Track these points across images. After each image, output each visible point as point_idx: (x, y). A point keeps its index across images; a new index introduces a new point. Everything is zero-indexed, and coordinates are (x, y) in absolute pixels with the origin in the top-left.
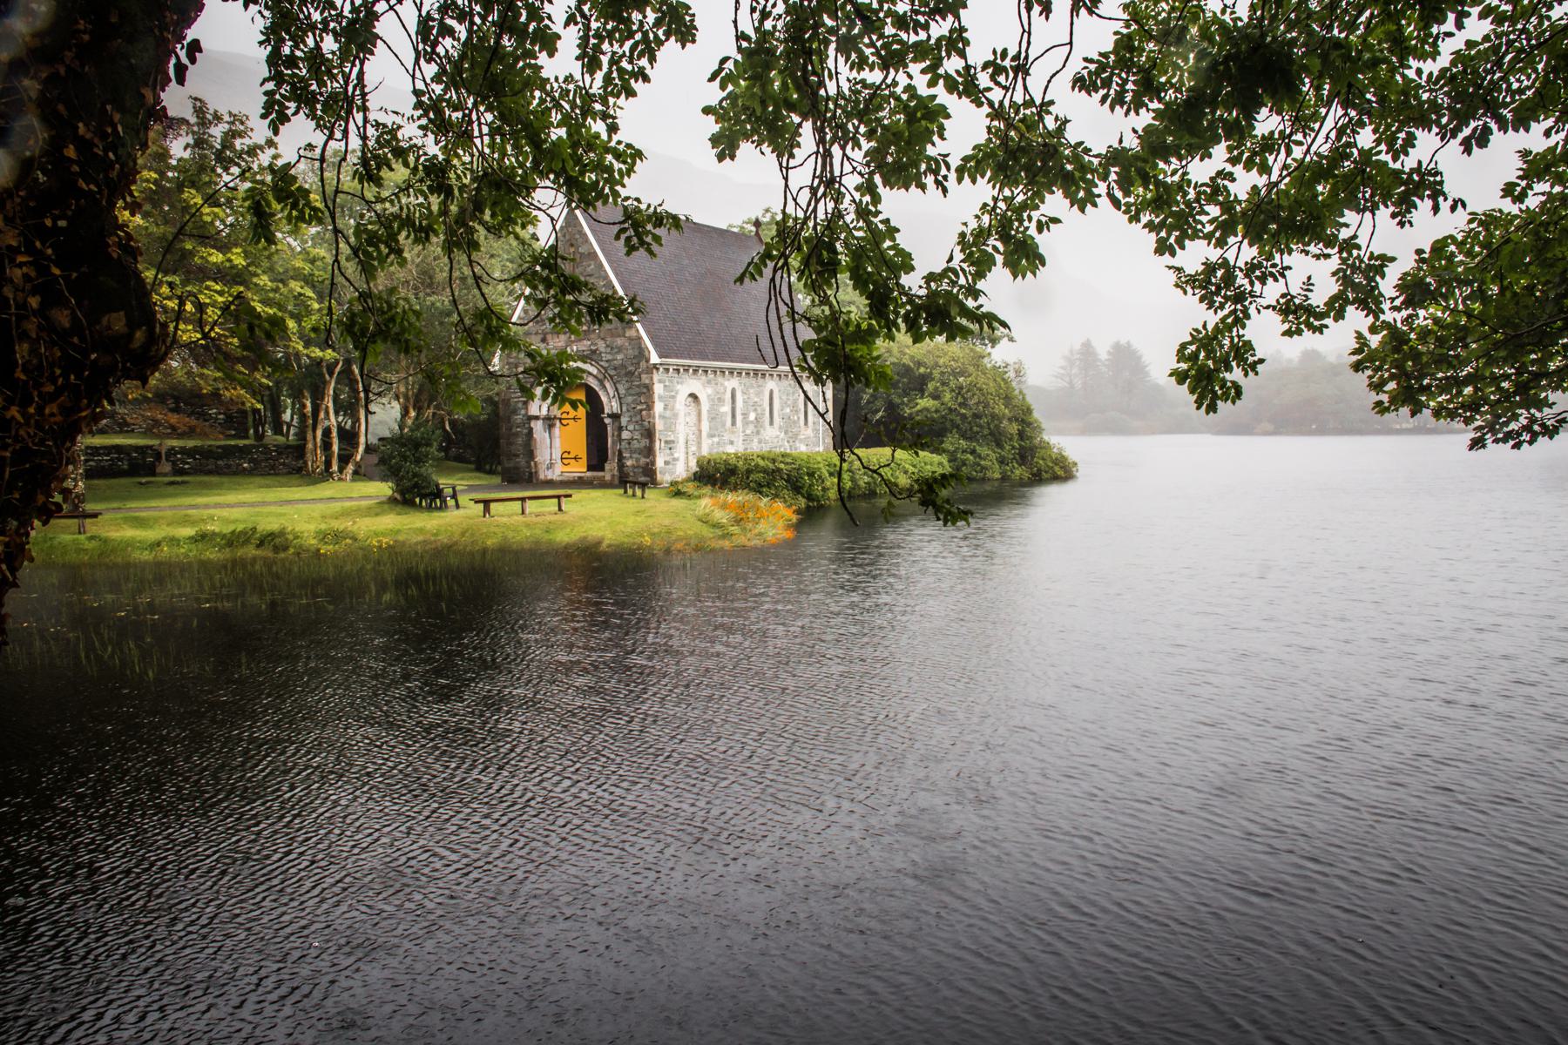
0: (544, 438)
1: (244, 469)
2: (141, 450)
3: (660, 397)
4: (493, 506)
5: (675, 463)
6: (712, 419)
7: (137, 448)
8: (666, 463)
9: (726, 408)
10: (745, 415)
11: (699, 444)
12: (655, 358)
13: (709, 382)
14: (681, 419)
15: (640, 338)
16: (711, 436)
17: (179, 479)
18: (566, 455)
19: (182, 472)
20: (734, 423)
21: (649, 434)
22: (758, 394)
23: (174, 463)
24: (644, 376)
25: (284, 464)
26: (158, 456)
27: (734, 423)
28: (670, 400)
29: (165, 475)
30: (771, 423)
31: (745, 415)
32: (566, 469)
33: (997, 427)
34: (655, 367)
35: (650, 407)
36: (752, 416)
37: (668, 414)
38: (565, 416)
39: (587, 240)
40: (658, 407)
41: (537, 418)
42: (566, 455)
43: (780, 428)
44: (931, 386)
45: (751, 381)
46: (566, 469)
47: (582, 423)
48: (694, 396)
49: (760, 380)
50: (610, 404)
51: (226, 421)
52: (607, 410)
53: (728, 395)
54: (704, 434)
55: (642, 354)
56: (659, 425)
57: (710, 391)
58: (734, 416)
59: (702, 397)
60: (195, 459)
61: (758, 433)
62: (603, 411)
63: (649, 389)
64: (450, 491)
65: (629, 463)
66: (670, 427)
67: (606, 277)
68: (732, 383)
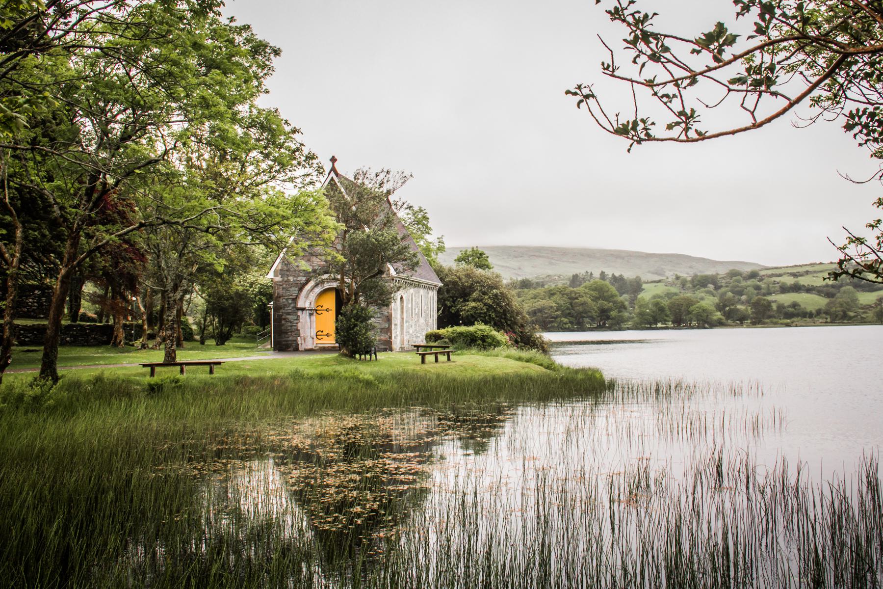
0: (306, 322)
1: (67, 342)
18: (320, 333)
25: (94, 338)
32: (319, 342)
33: (515, 319)
38: (320, 308)
41: (303, 309)
42: (320, 333)
44: (475, 295)
46: (319, 342)
47: (333, 314)
48: (402, 298)
51: (38, 308)
60: (33, 334)
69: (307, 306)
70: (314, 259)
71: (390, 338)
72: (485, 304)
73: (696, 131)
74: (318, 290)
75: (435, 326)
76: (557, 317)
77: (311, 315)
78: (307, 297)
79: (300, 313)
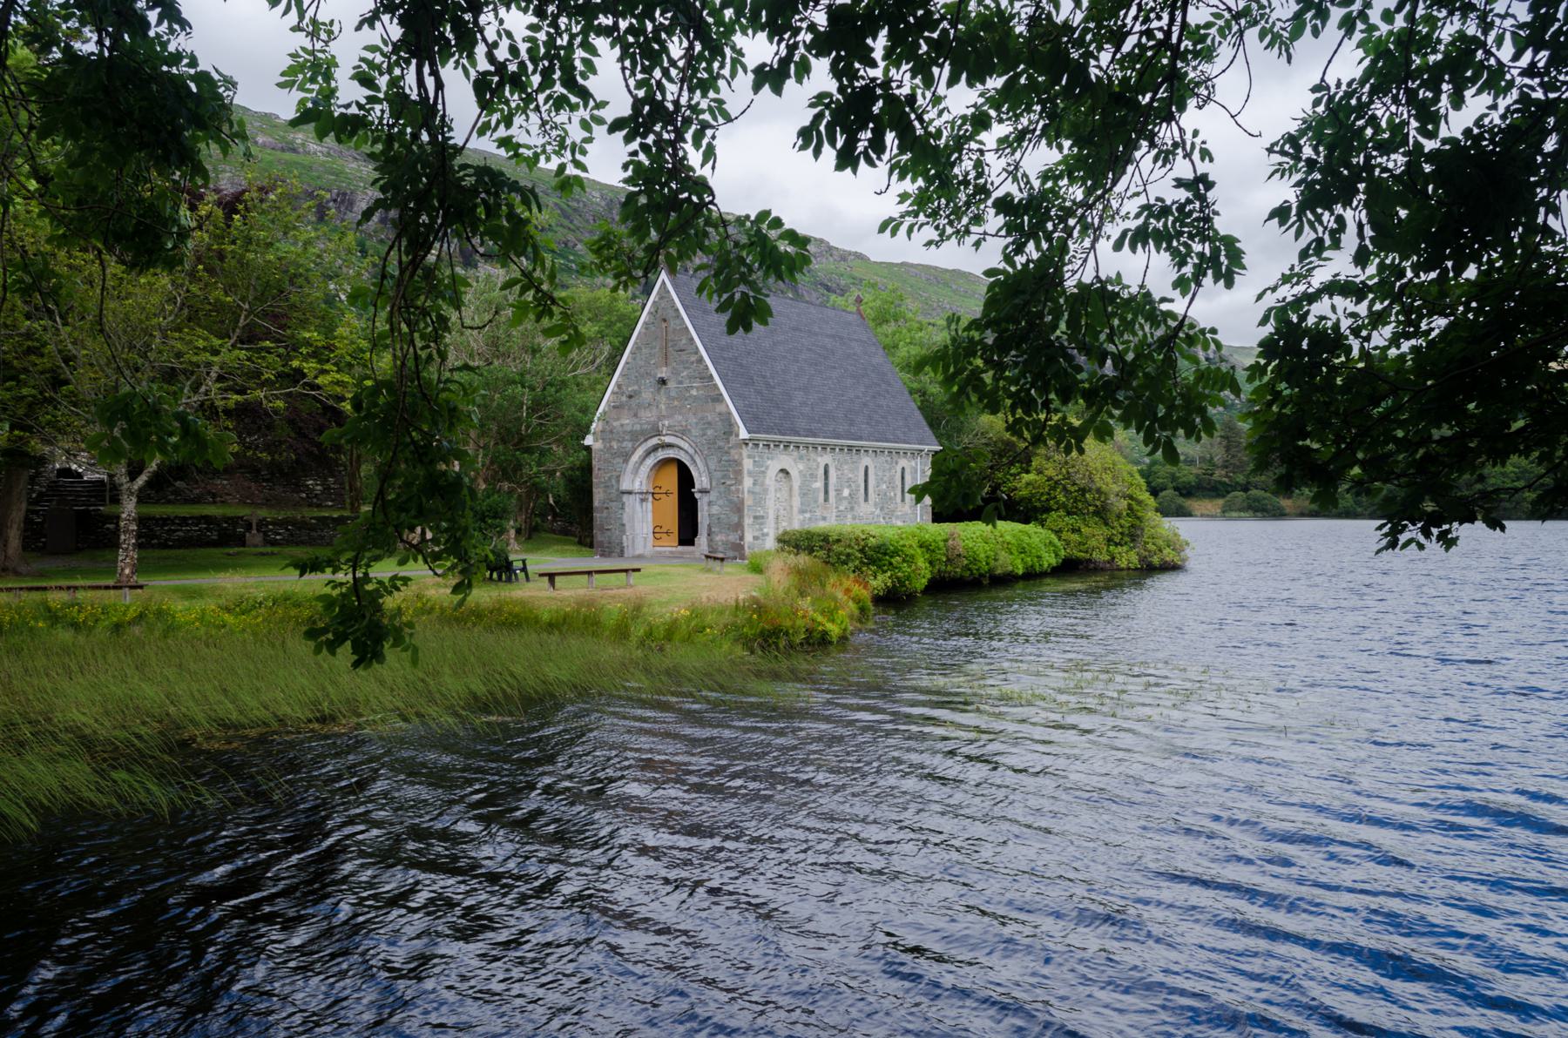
2: (234, 521)
3: (750, 473)
4: (557, 579)
5: (762, 536)
6: (804, 495)
7: (227, 519)
8: (755, 538)
9: (819, 484)
10: (839, 491)
11: (790, 520)
12: (743, 434)
13: (801, 458)
14: (771, 495)
15: (730, 413)
16: (802, 511)
17: (269, 549)
19: (274, 543)
20: (826, 500)
21: (739, 508)
22: (851, 471)
23: (265, 534)
24: (733, 452)
26: (249, 527)
27: (826, 500)
28: (759, 476)
29: (256, 546)
30: (866, 500)
31: (839, 491)
34: (745, 443)
35: (739, 481)
36: (846, 492)
37: (757, 489)
39: (678, 316)
40: (748, 482)
41: (630, 493)
43: (876, 505)
45: (845, 456)
47: (674, 499)
49: (855, 457)
50: (701, 480)
52: (698, 486)
53: (821, 471)
54: (795, 510)
55: (730, 430)
56: (748, 501)
57: (801, 467)
58: (826, 492)
59: (794, 473)
61: (852, 509)
62: (693, 486)
63: (738, 463)
64: (520, 564)
65: (718, 538)
66: (760, 501)
67: (697, 351)
68: (825, 459)
69: (637, 487)
70: (642, 413)
71: (742, 538)
72: (1050, 479)
73: (702, 166)
74: (650, 461)
75: (930, 517)
76: (1517, 490)
77: (642, 500)
78: (636, 471)
79: (625, 498)
